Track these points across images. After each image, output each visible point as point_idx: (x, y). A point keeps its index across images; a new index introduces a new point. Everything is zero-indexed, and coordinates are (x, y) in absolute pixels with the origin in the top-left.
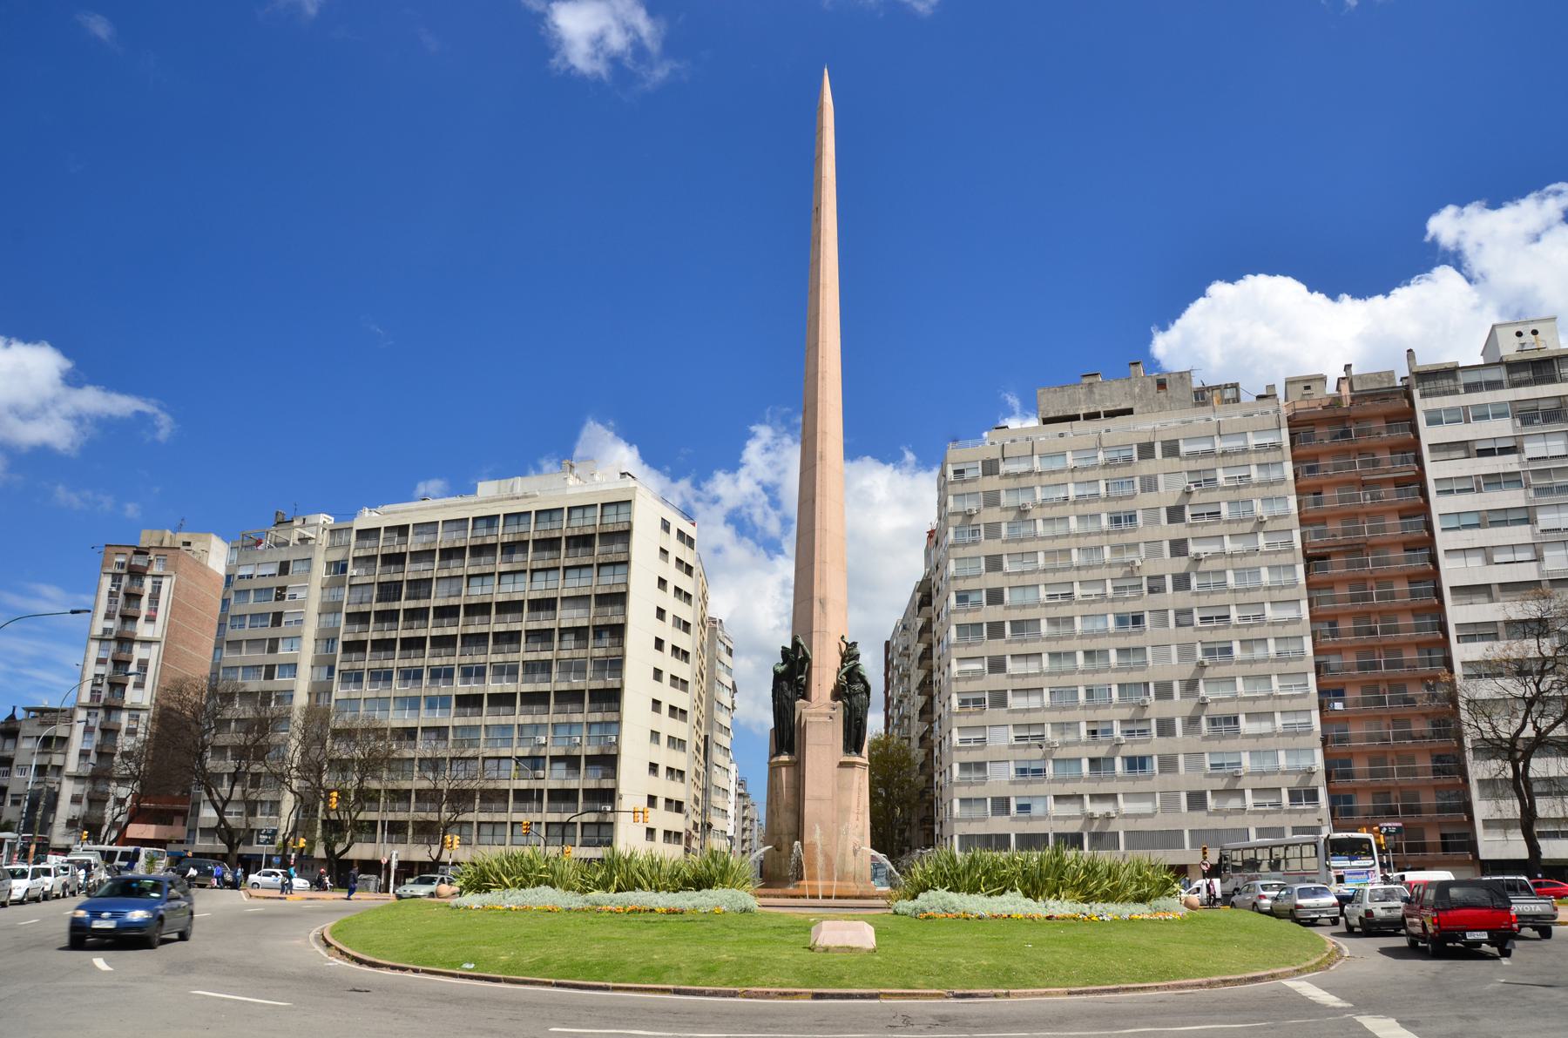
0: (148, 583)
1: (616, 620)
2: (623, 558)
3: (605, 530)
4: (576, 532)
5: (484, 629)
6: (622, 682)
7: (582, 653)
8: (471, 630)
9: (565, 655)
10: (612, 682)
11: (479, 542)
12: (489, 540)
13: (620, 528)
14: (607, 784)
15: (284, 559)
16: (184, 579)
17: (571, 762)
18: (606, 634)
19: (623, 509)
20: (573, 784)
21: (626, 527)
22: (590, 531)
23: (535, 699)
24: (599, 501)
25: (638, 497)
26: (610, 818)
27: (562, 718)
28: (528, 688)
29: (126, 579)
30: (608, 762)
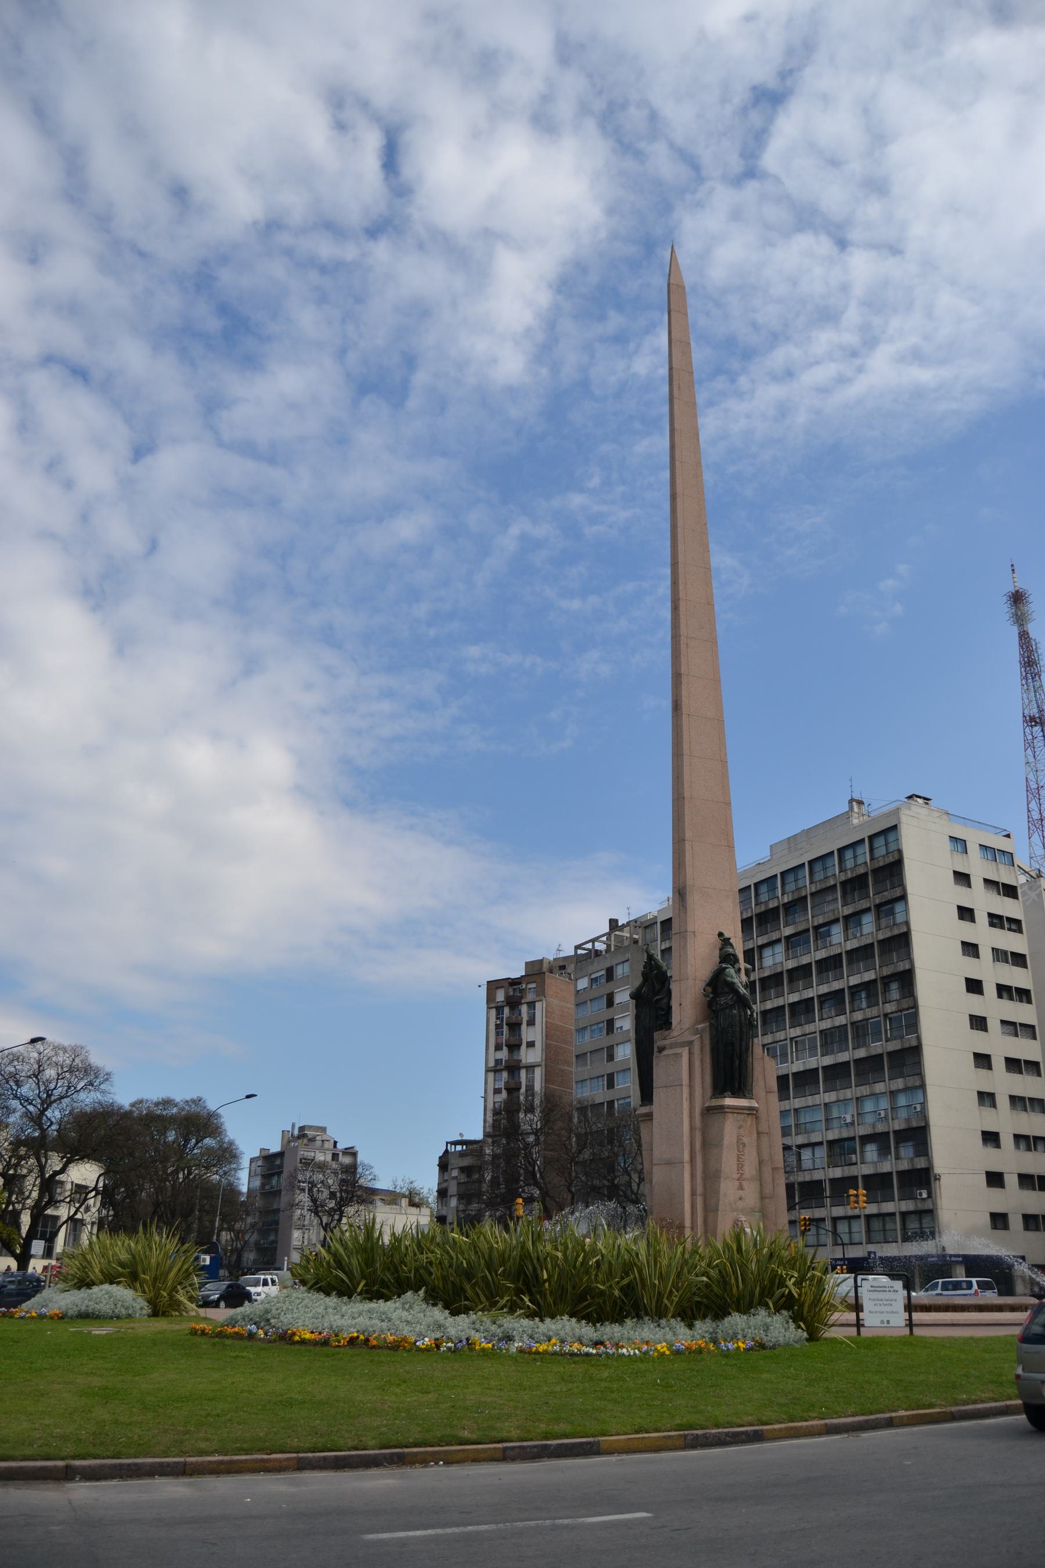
0: (524, 1009)
1: (903, 966)
2: (898, 892)
3: (877, 866)
4: (849, 875)
5: (779, 1002)
6: (919, 1038)
7: (874, 1011)
8: (769, 1005)
9: (858, 1016)
10: (910, 1040)
11: (763, 908)
12: (773, 904)
13: (891, 859)
14: (921, 1163)
15: (608, 965)
16: (555, 1002)
17: (880, 1139)
18: (894, 986)
19: (891, 837)
20: (886, 1166)
21: (897, 857)
22: (861, 870)
23: (837, 1074)
24: (865, 834)
25: (904, 819)
26: (929, 1205)
27: (864, 1090)
28: (828, 1061)
29: (506, 1010)
30: (918, 1136)
